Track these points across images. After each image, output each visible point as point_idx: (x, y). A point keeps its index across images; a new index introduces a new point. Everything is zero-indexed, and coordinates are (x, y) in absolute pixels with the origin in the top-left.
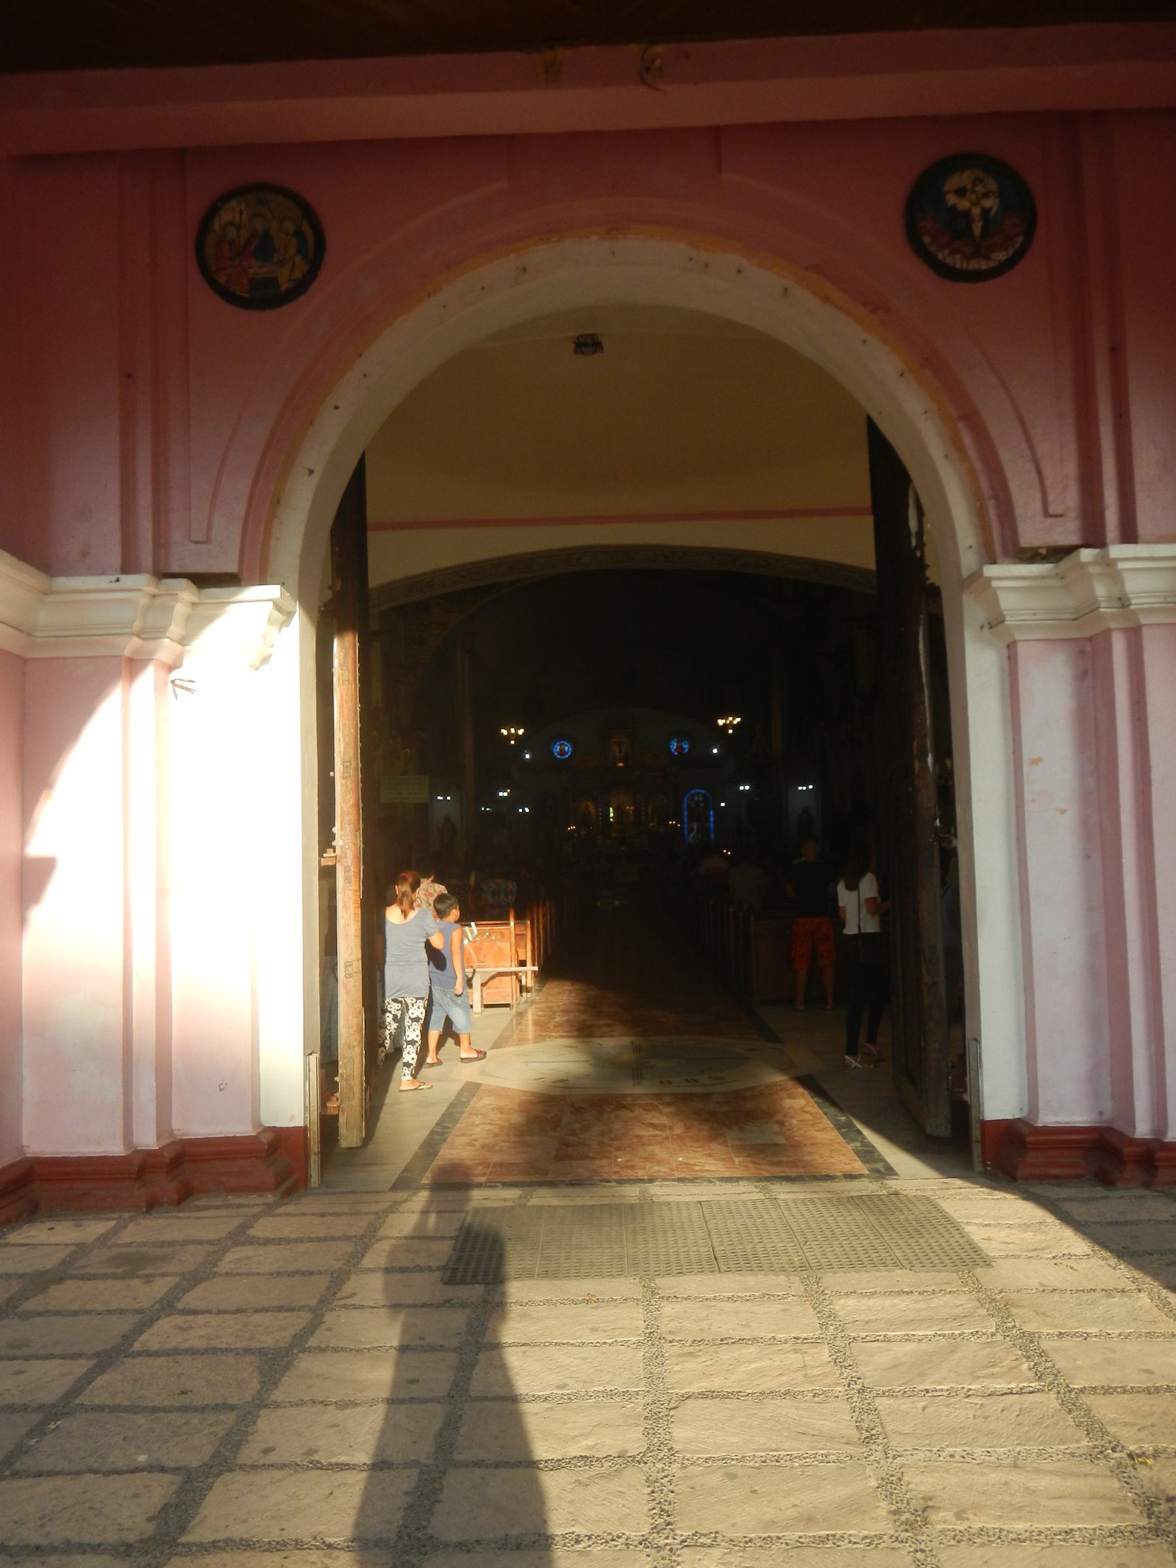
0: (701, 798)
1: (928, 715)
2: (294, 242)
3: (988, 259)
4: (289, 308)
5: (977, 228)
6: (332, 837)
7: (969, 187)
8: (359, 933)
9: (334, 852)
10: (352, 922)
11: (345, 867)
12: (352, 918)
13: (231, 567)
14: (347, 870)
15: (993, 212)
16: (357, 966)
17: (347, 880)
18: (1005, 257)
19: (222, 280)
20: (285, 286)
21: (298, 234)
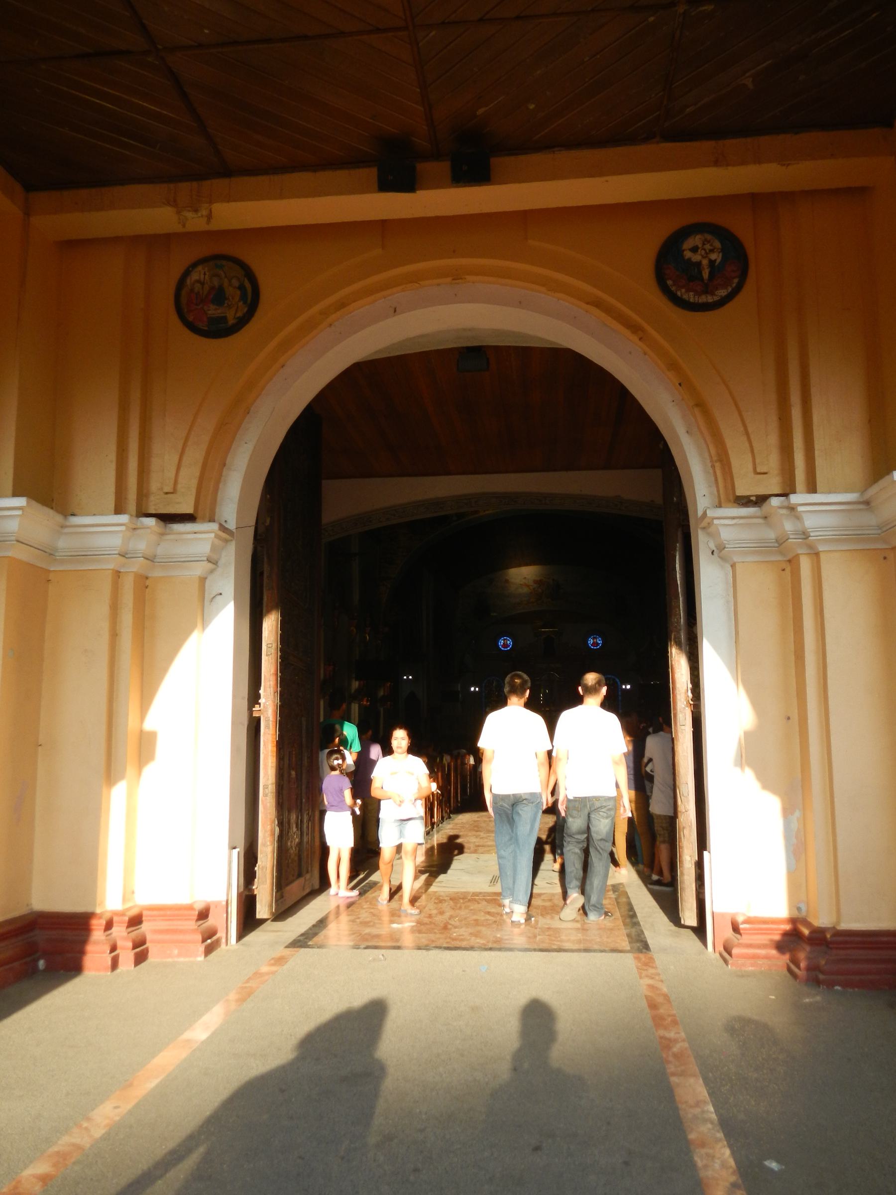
0: (612, 682)
1: (682, 615)
2: (238, 292)
3: (713, 294)
5: (706, 274)
6: (258, 696)
7: (700, 246)
8: (274, 764)
9: (260, 707)
10: (270, 756)
11: (266, 718)
12: (270, 754)
13: (188, 509)
14: (267, 721)
15: (718, 261)
17: (267, 727)
18: (726, 293)
19: (191, 318)
20: (231, 321)
21: (242, 288)
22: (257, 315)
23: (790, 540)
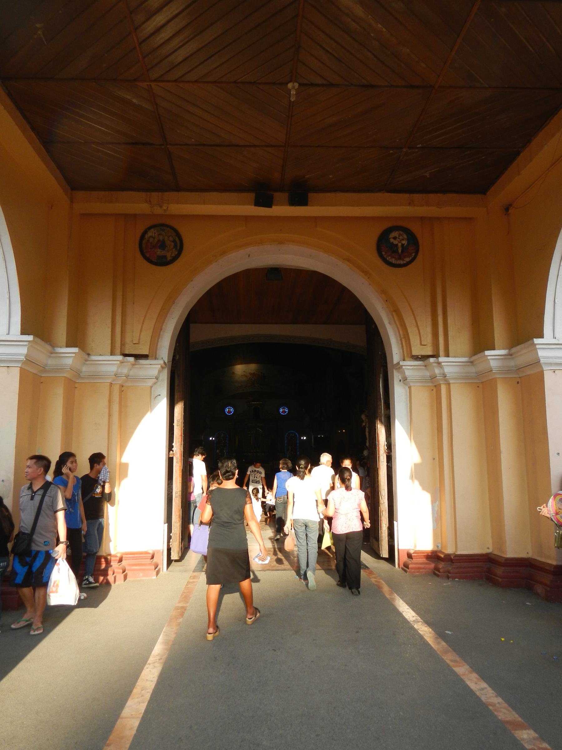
0: (293, 435)
2: (173, 244)
3: (403, 260)
4: (171, 266)
6: (173, 447)
7: (397, 236)
8: (181, 481)
9: (173, 452)
12: (178, 476)
13: (146, 352)
15: (406, 244)
16: (179, 493)
17: (177, 462)
18: (409, 260)
19: (148, 256)
20: (169, 258)
21: (174, 241)
22: (182, 256)
23: (437, 378)
